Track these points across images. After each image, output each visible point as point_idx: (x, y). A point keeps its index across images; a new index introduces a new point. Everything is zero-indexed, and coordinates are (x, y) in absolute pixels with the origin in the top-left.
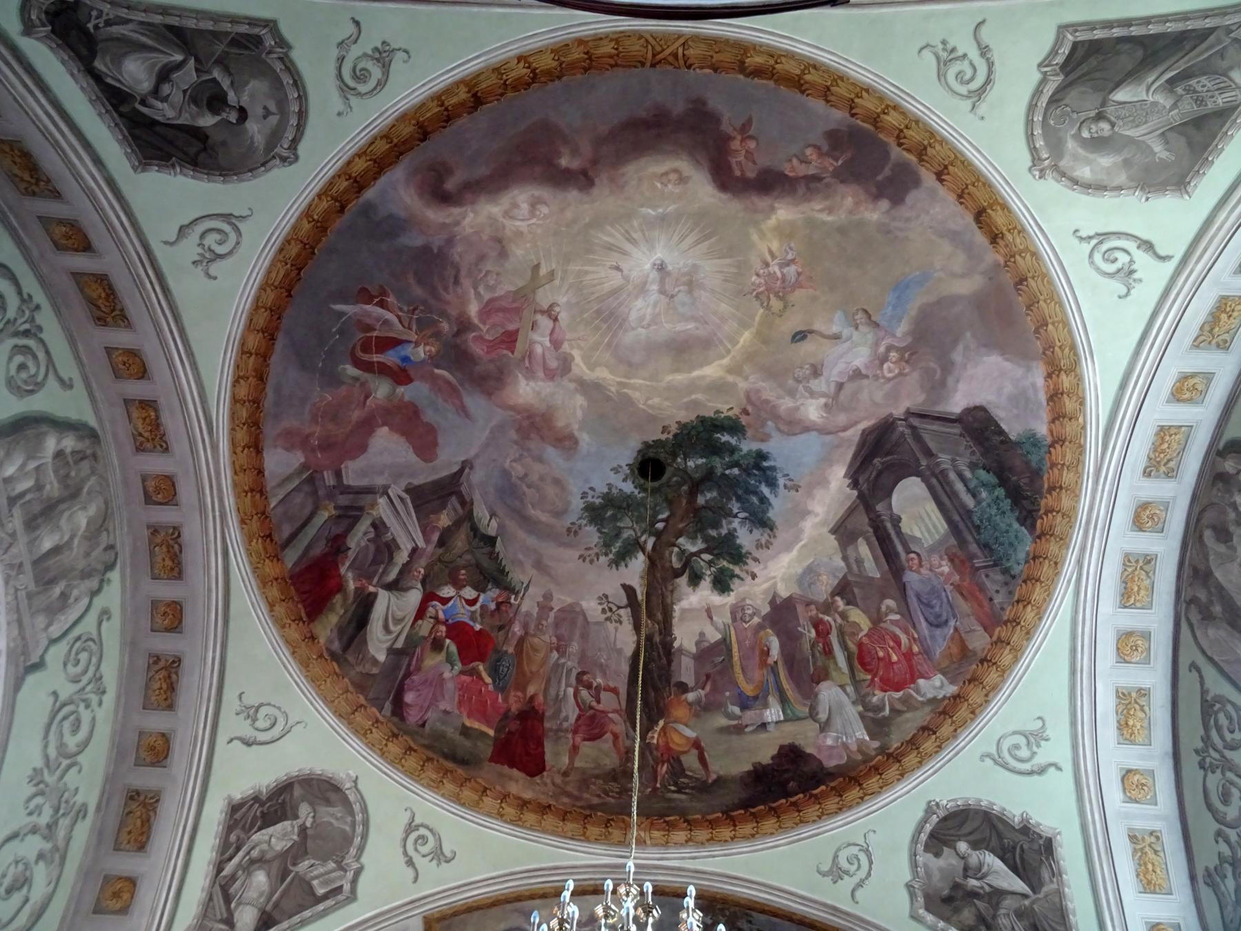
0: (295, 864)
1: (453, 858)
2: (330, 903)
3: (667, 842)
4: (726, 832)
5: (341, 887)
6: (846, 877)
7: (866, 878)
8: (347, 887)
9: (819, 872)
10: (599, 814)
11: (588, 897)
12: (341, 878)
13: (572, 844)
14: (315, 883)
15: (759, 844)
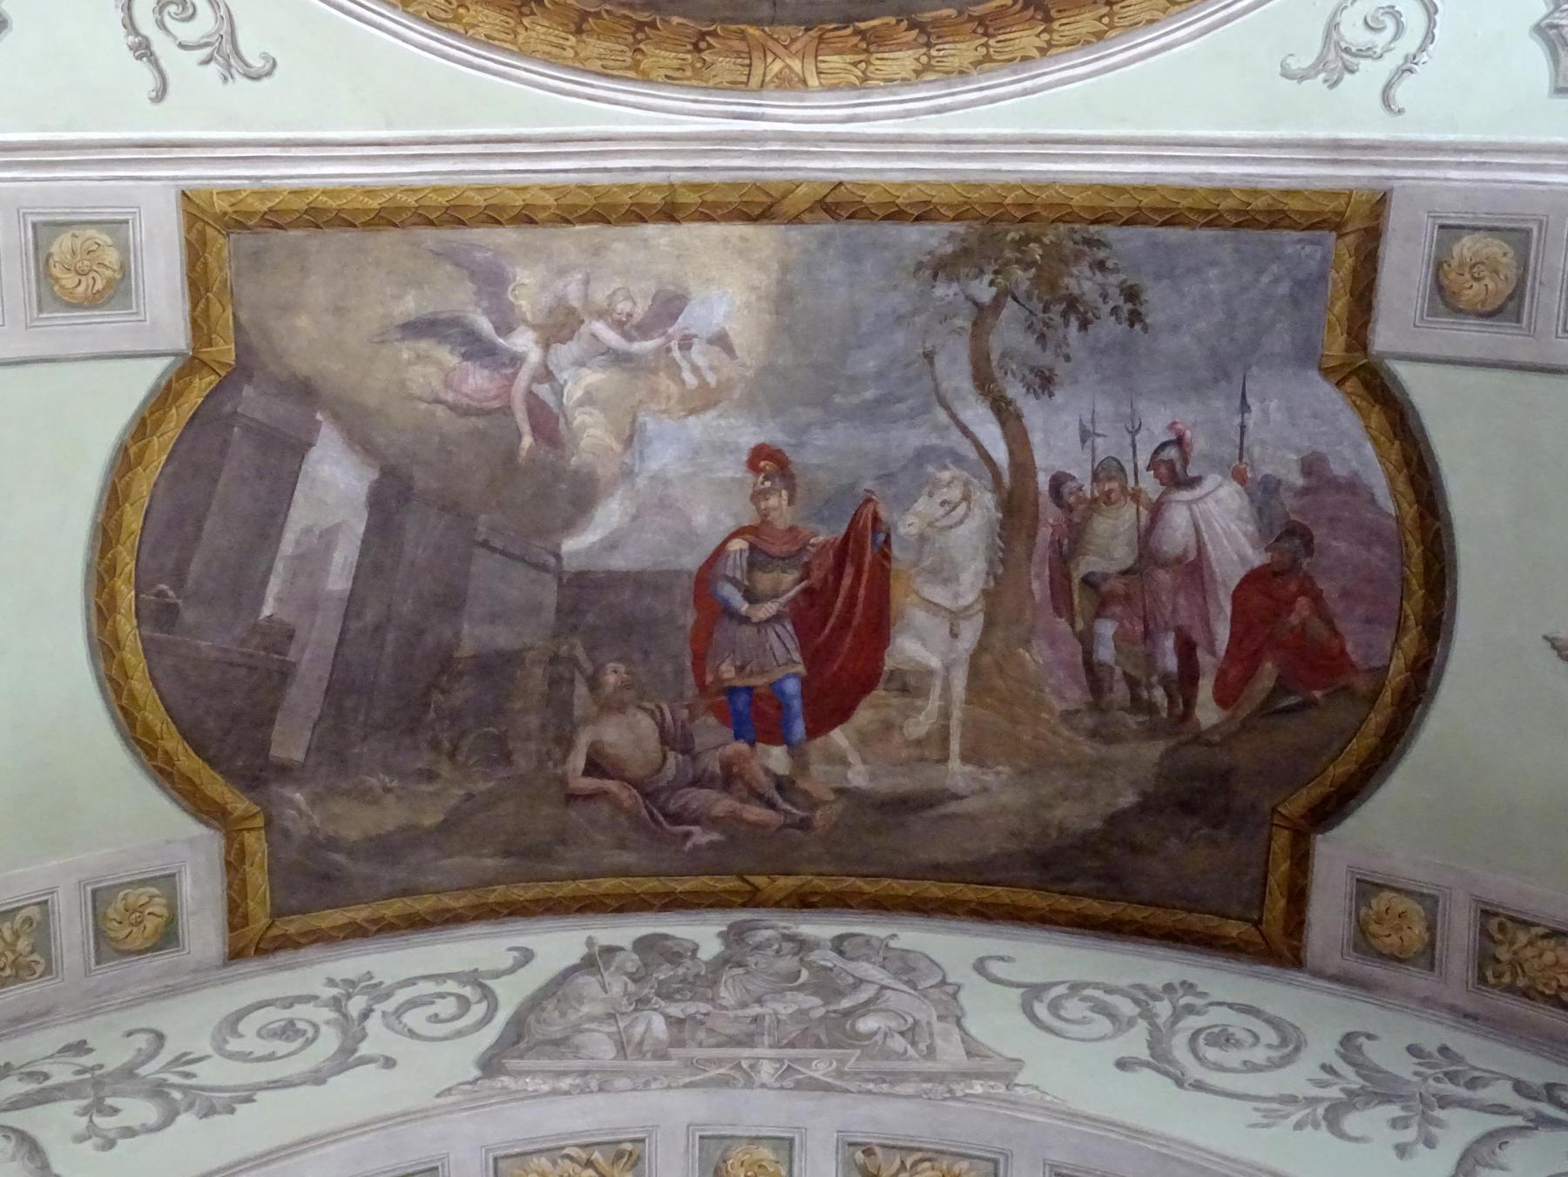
1: (269, 74)
3: (865, 79)
4: (1027, 39)
6: (1364, 64)
7: (1422, 49)
9: (1286, 74)
10: (676, 20)
11: (651, 229)
13: (602, 87)
15: (1116, 52)
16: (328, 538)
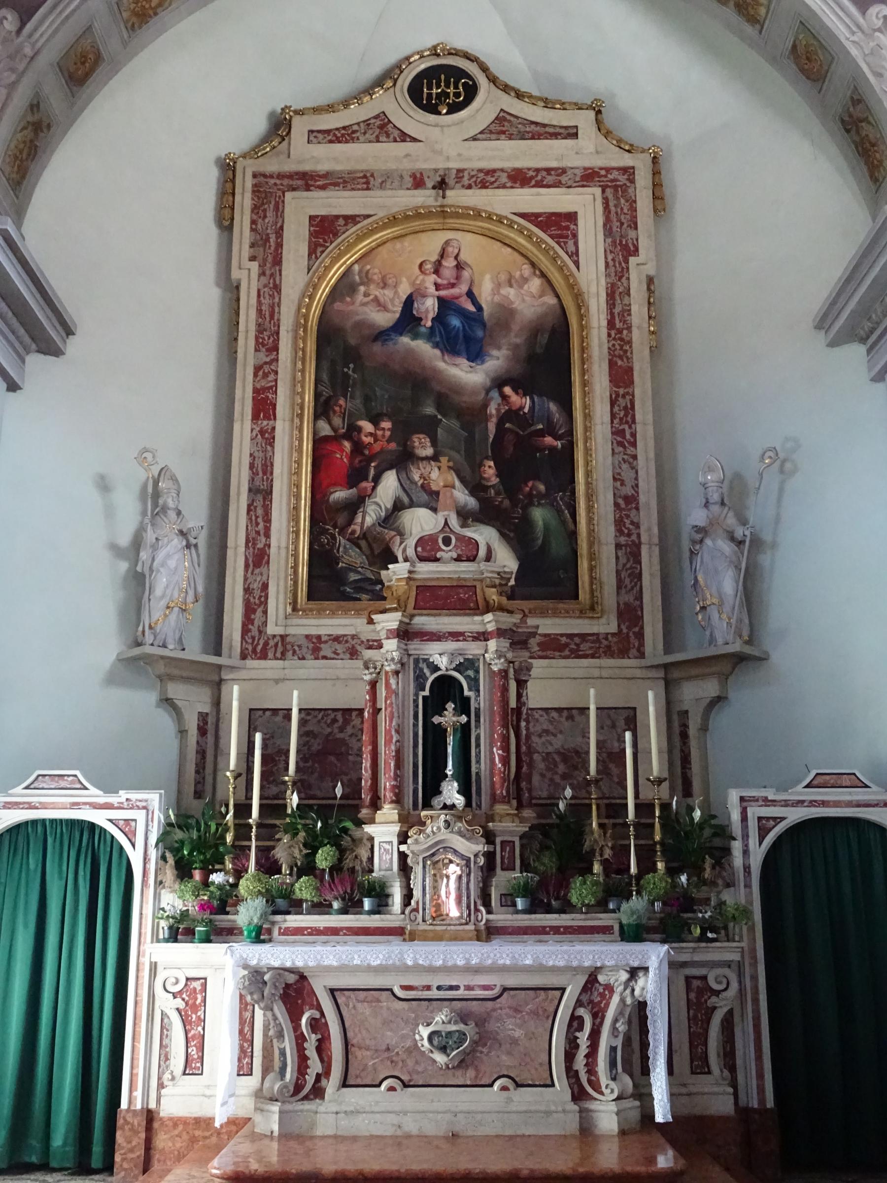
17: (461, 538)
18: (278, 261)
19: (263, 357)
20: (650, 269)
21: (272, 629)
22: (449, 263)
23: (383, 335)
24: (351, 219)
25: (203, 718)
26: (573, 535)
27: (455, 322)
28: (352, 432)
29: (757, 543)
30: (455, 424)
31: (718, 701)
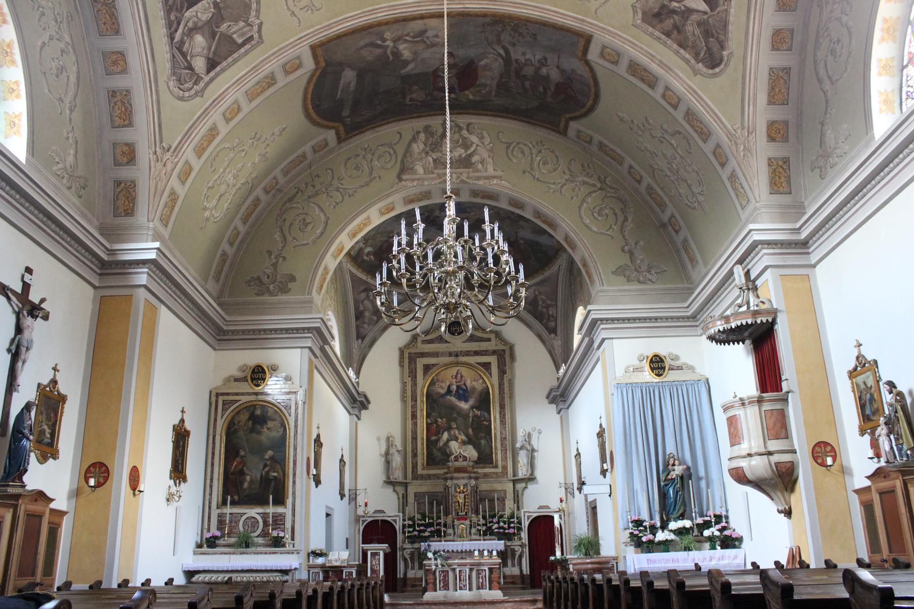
0: (218, 27)
2: (248, 46)
5: (252, 36)
8: (256, 36)
12: (251, 30)
14: (235, 36)
16: (349, 83)
17: (464, 456)
18: (416, 377)
19: (413, 403)
20: (510, 377)
21: (419, 473)
22: (459, 376)
23: (443, 396)
24: (434, 365)
25: (403, 494)
26: (491, 447)
27: (461, 392)
28: (436, 421)
29: (533, 450)
30: (461, 419)
31: (526, 488)
